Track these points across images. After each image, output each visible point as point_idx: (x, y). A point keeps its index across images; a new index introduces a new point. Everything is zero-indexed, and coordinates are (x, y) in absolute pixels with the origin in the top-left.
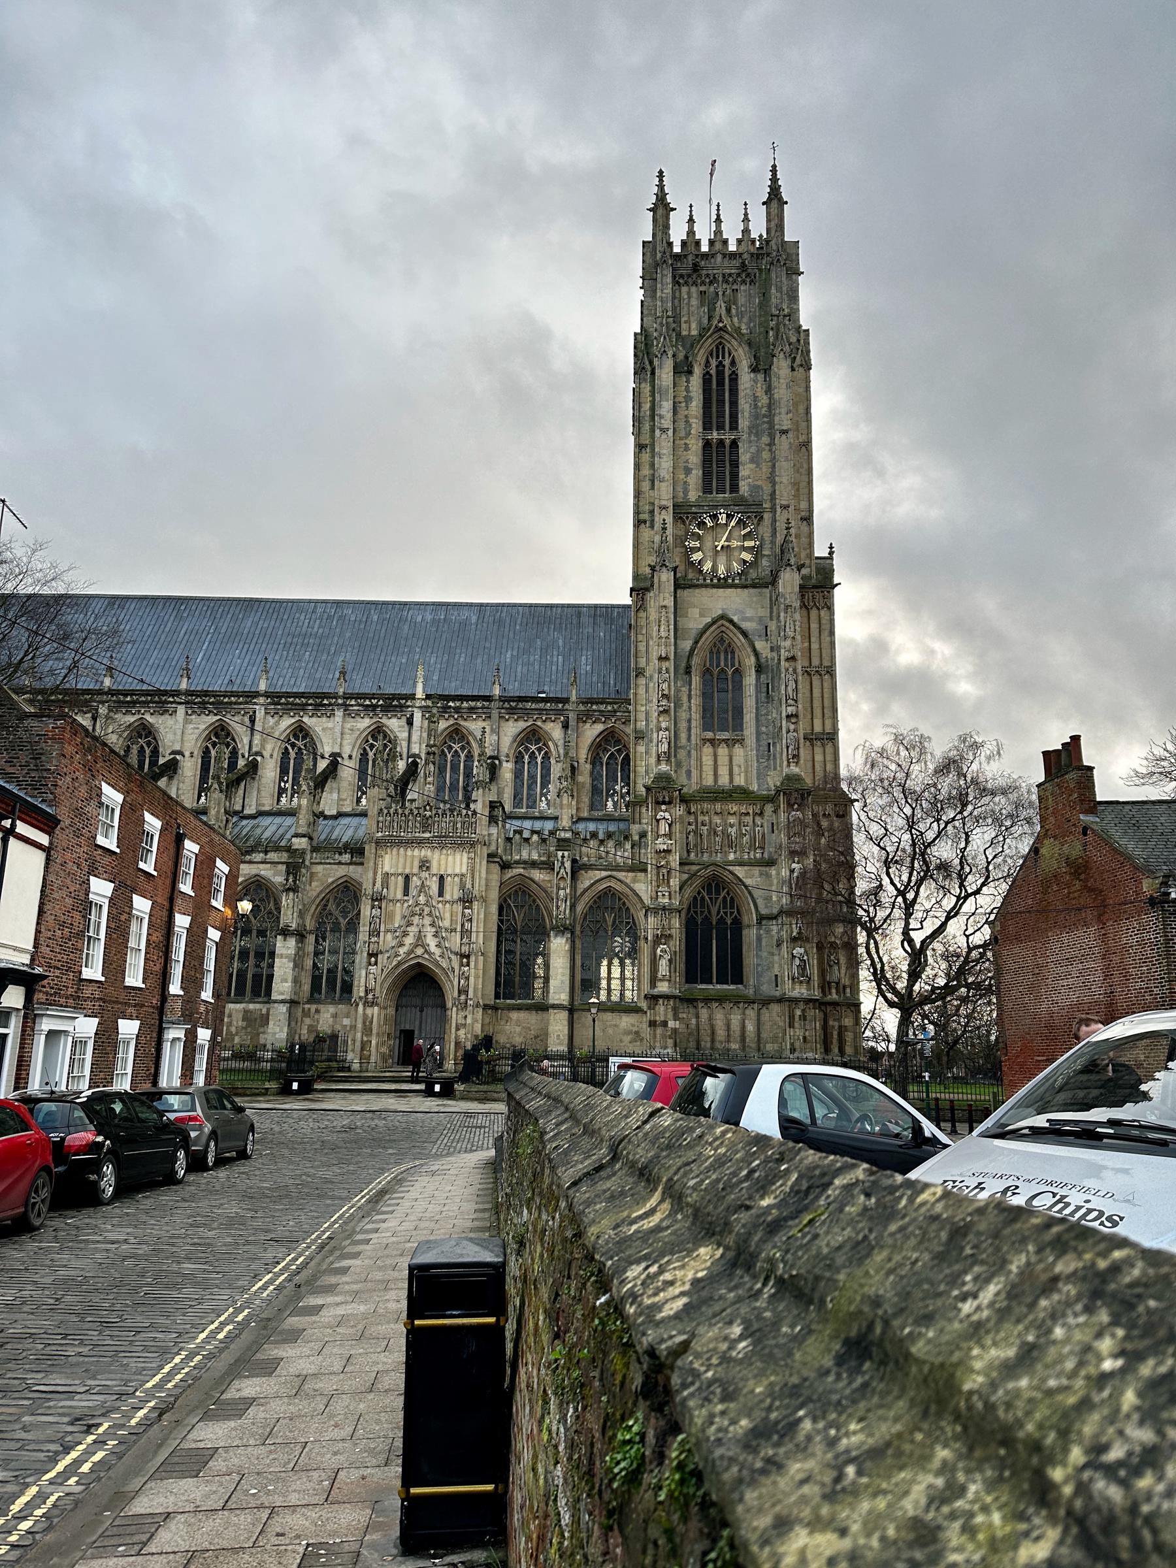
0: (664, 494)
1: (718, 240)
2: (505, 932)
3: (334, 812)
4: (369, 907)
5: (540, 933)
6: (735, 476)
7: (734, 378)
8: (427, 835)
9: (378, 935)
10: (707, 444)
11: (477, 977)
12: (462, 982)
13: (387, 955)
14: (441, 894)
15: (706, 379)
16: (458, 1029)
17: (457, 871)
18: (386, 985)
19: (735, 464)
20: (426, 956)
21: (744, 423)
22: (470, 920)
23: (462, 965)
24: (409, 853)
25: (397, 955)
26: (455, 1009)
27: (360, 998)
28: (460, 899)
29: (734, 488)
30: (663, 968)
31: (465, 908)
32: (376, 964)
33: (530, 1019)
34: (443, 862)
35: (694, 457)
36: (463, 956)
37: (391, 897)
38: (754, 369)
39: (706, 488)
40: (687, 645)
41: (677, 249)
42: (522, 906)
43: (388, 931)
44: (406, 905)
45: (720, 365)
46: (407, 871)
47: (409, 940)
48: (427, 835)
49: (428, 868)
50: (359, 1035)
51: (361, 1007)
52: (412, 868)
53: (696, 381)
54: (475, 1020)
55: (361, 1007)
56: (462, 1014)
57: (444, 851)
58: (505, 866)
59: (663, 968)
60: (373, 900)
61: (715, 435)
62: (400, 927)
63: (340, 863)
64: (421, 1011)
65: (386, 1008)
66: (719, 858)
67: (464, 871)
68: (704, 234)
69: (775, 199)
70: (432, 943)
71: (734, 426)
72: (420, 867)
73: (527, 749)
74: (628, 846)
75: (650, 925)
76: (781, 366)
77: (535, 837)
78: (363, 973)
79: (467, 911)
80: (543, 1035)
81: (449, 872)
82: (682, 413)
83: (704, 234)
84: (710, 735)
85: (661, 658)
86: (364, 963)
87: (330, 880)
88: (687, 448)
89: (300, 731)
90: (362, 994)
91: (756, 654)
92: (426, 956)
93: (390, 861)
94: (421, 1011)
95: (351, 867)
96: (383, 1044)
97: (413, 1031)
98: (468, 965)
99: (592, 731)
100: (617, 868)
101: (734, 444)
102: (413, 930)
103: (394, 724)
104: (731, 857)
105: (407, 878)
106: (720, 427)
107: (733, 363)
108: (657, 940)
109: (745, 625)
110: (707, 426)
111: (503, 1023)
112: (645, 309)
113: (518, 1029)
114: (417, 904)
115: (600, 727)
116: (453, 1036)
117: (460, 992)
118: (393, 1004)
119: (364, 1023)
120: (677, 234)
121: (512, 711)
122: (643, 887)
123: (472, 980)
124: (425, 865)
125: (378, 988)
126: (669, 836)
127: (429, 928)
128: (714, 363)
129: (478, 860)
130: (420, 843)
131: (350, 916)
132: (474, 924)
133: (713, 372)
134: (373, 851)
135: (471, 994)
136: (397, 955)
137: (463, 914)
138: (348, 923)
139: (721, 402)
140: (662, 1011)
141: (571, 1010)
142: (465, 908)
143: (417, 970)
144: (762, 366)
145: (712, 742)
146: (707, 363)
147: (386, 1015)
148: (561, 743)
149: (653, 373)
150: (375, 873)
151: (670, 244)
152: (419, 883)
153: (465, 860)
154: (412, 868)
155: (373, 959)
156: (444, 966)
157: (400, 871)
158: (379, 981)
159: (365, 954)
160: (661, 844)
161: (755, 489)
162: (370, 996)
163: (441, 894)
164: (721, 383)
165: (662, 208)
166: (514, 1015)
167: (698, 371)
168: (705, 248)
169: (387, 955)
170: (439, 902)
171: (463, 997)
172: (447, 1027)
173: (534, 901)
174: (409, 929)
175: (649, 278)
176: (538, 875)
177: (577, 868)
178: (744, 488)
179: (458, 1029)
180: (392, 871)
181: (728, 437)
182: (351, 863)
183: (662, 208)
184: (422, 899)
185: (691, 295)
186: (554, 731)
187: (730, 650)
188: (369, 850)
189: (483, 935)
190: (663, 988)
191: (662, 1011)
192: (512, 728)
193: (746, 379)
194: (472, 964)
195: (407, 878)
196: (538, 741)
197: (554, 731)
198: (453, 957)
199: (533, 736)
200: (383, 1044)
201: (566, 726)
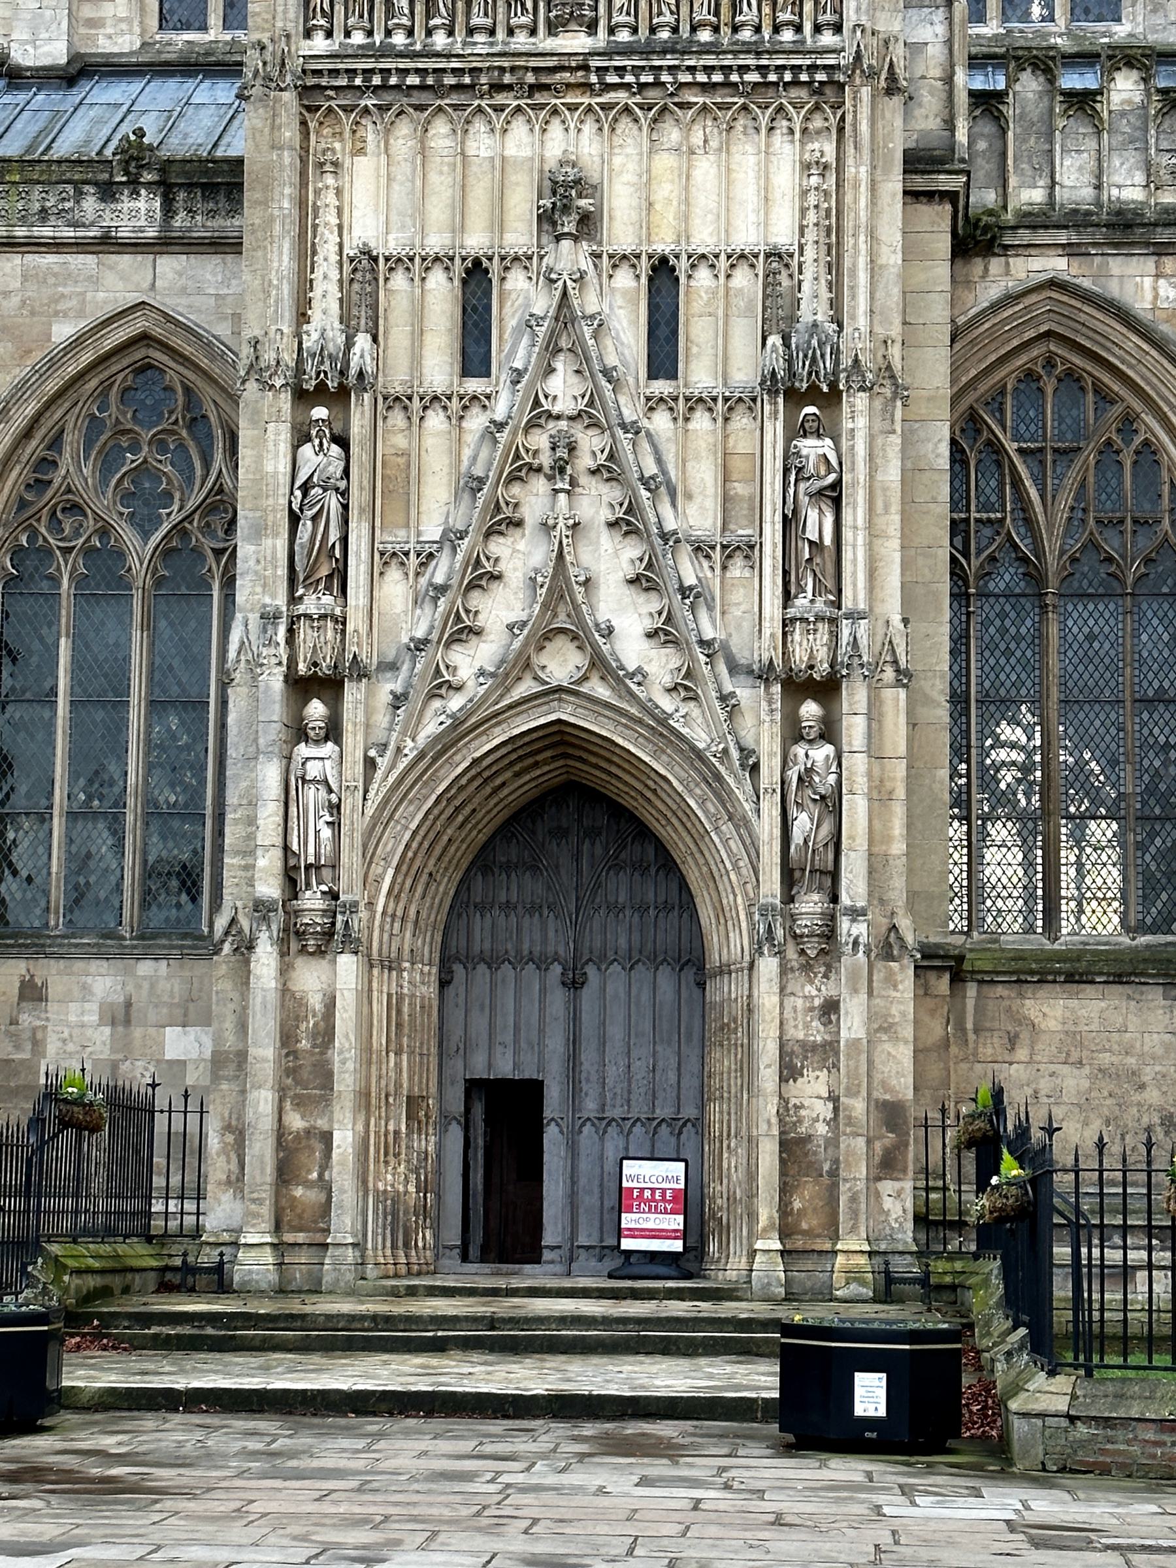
3: (54, 52)
4: (280, 435)
8: (575, 42)
9: (339, 579)
11: (879, 797)
12: (802, 823)
13: (387, 687)
16: (789, 1072)
17: (746, 237)
18: (394, 843)
20: (601, 690)
22: (833, 496)
23: (794, 733)
24: (481, 142)
25: (442, 687)
26: (768, 966)
27: (262, 909)
28: (770, 383)
31: (797, 430)
32: (333, 731)
34: (666, 191)
37: (396, 379)
42: (1066, 454)
43: (389, 558)
44: (476, 422)
46: (476, 242)
48: (575, 42)
49: (588, 224)
50: (263, 1102)
51: (265, 959)
52: (499, 224)
54: (880, 1026)
55: (265, 959)
56: (814, 991)
57: (671, 134)
60: (303, 397)
62: (452, 538)
63: (107, 244)
64: (574, 983)
65: (391, 965)
67: (783, 235)
72: (547, 219)
78: (270, 775)
79: (812, 448)
81: (704, 239)
86: (273, 731)
87: (63, 331)
90: (270, 888)
92: (601, 690)
94: (574, 983)
95: (169, 265)
96: (390, 1149)
97: (533, 1090)
98: (829, 732)
111: (991, 1047)
113: (1074, 1081)
114: (539, 417)
116: (769, 1108)
117: (790, 877)
118: (428, 946)
119: (287, 1038)
123: (856, 810)
125: (351, 859)
127: (607, 541)
129: (858, 170)
131: (172, 515)
132: (855, 514)
134: (290, 133)
136: (442, 687)
137: (792, 467)
138: (166, 553)
142: (797, 430)
143: (548, 773)
147: (395, 1004)
150: (305, 254)
152: (543, 303)
153: (785, 177)
154: (499, 224)
155: (316, 709)
156: (700, 737)
157: (436, 242)
158: (355, 819)
159: (274, 681)
162: (312, 900)
169: (387, 687)
170: (653, 404)
171: (810, 905)
172: (723, 1062)
173: (1128, 422)
174: (499, 547)
179: (789, 1072)
180: (393, 245)
182: (165, 244)
194: (854, 730)
198: (745, 693)
200: (390, 1149)
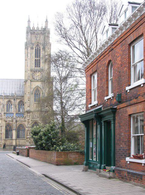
0: (29, 69)
5: (11, 130)
6: (40, 65)
10: (36, 60)
15: (36, 49)
19: (40, 63)
29: (40, 67)
30: (28, 134)
33: (11, 141)
35: (34, 62)
38: (43, 49)
39: (36, 67)
40: (32, 90)
41: (31, 29)
45: (38, 48)
59: (28, 134)
61: (37, 59)
66: (36, 120)
71: (40, 57)
73: (8, 103)
74: (24, 118)
75: (27, 129)
80: (12, 143)
82: (32, 55)
84: (35, 102)
85: (28, 93)
99: (18, 101)
100: (23, 121)
101: (40, 60)
104: (38, 119)
106: (38, 57)
107: (40, 48)
108: (28, 131)
110: (36, 57)
112: (27, 39)
115: (19, 100)
121: (6, 98)
122: (26, 123)
126: (29, 117)
128: (37, 47)
133: (37, 49)
139: (38, 54)
140: (28, 139)
141: (16, 140)
148: (13, 102)
149: (27, 49)
151: (30, 28)
160: (28, 118)
161: (43, 67)
164: (38, 51)
166: (8, 141)
175: (27, 33)
176: (11, 122)
181: (39, 59)
185: (33, 36)
186: (13, 101)
187: (39, 91)
190: (28, 137)
191: (28, 139)
192: (6, 100)
193: (41, 50)
196: (10, 102)
197: (13, 101)
199: (9, 101)
201: (14, 100)
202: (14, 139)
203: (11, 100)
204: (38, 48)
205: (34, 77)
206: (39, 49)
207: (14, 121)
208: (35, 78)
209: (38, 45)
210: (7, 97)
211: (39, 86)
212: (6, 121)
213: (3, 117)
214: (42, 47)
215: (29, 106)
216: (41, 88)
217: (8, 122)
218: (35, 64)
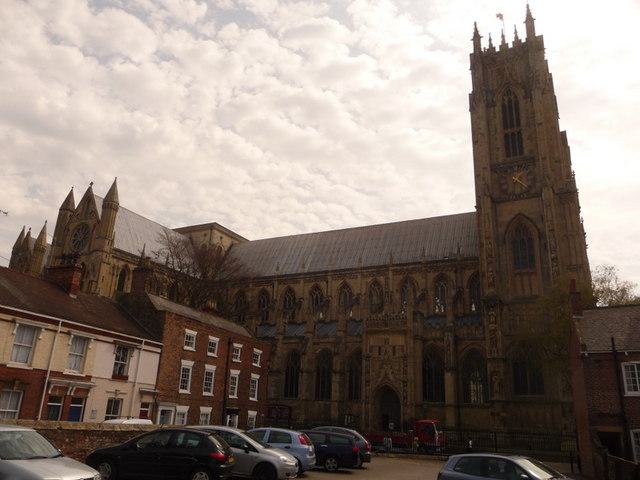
1: (504, 45)
2: (426, 373)
7: (517, 103)
10: (506, 136)
14: (394, 355)
15: (503, 106)
21: (523, 121)
29: (521, 152)
35: (500, 143)
36: (404, 382)
38: (525, 97)
47: (382, 375)
53: (498, 108)
58: (424, 341)
68: (497, 45)
69: (530, 22)
70: (391, 377)
71: (519, 124)
76: (537, 95)
77: (438, 327)
83: (497, 45)
88: (496, 139)
89: (345, 285)
91: (539, 230)
93: (373, 341)
102: (383, 371)
103: (382, 279)
105: (380, 348)
107: (516, 97)
109: (531, 216)
110: (505, 126)
120: (485, 45)
124: (386, 341)
130: (385, 332)
135: (409, 398)
144: (528, 96)
145: (520, 274)
146: (503, 100)
160: (492, 327)
161: (531, 151)
163: (394, 355)
164: (510, 107)
165: (477, 38)
167: (499, 104)
168: (497, 50)
176: (440, 344)
177: (457, 340)
178: (526, 152)
181: (516, 129)
183: (477, 38)
184: (386, 357)
186: (452, 275)
188: (364, 336)
189: (414, 374)
192: (432, 276)
193: (522, 103)
195: (380, 348)
201: (456, 272)
202: (450, 406)
203: (448, 273)
204: (510, 101)
205: (505, 187)
206: (513, 102)
207: (449, 337)
208: (510, 190)
209: (508, 92)
210: (432, 265)
211: (526, 214)
212: (424, 341)
213: (410, 325)
214: (520, 93)
215: (491, 285)
216: (531, 221)
217: (429, 343)
218: (507, 148)
